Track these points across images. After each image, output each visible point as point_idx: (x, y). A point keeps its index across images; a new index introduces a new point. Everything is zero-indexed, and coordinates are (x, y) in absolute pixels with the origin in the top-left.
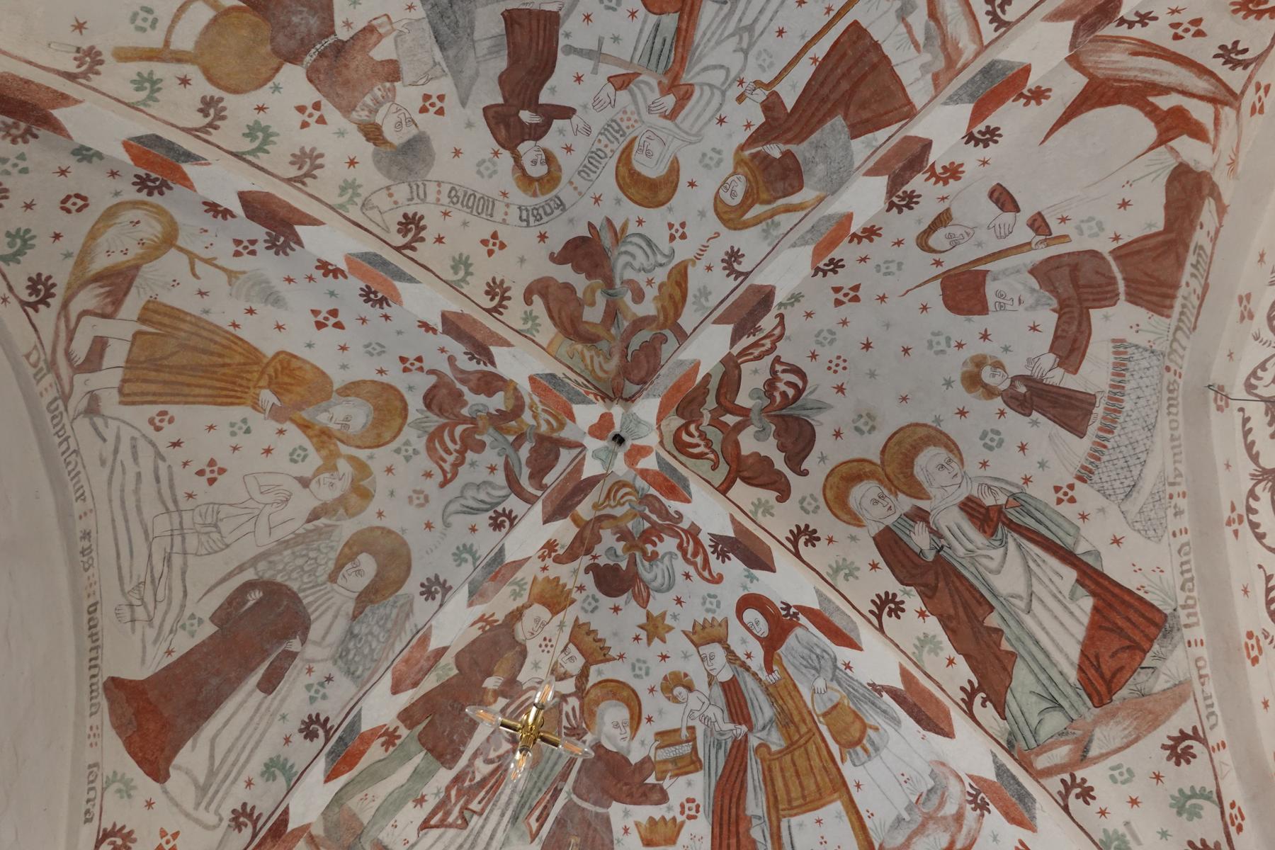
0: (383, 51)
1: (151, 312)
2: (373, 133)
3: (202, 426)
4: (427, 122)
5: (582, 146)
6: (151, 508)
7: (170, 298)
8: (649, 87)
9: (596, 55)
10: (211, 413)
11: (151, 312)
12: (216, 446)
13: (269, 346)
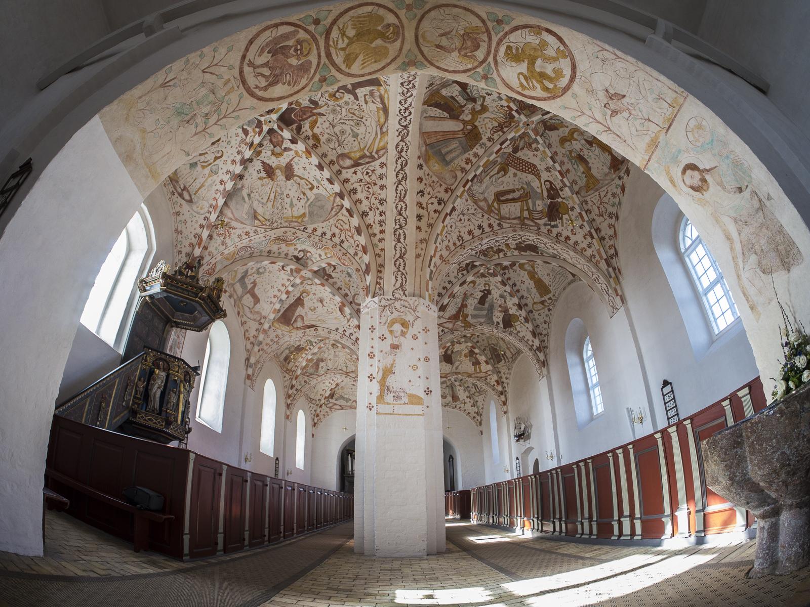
0: (500, 309)
1: (542, 297)
2: (505, 302)
3: (546, 280)
4: (498, 298)
5: (480, 287)
6: (557, 280)
7: (539, 296)
8: (469, 293)
9: (474, 298)
10: (544, 281)
11: (542, 297)
12: (546, 276)
13: (532, 282)
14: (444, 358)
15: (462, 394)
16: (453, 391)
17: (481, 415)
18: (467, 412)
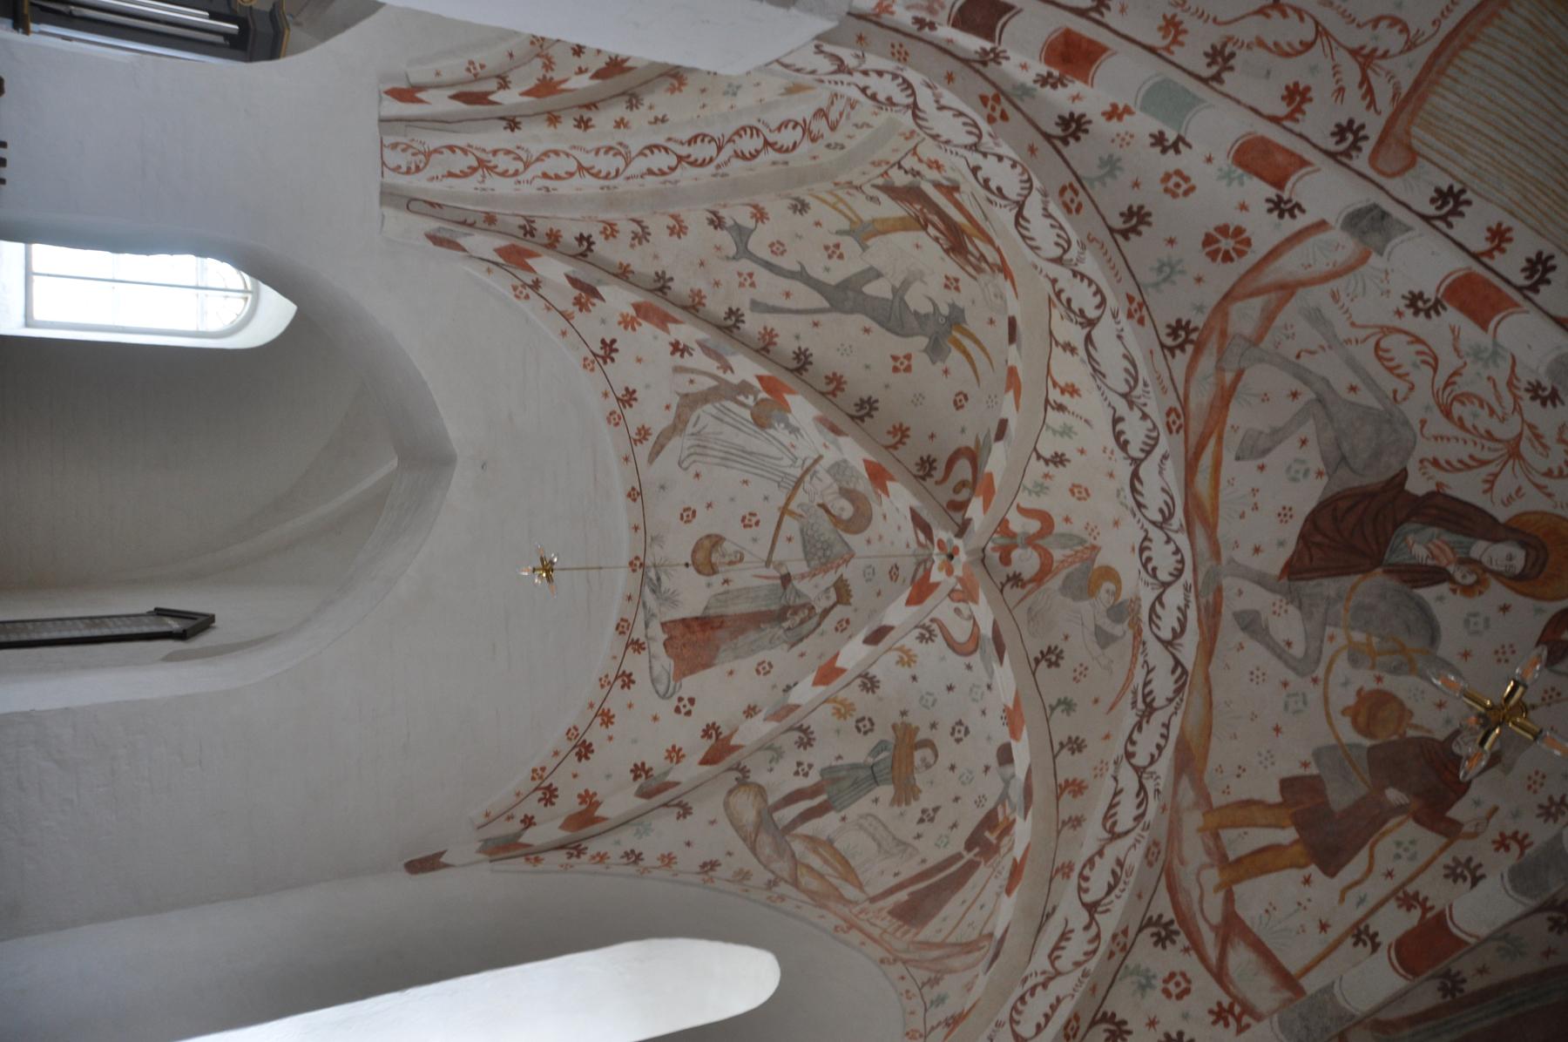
14: (1363, 496)
15: (726, 689)
16: (756, 620)
17: (574, 849)
18: (596, 735)
